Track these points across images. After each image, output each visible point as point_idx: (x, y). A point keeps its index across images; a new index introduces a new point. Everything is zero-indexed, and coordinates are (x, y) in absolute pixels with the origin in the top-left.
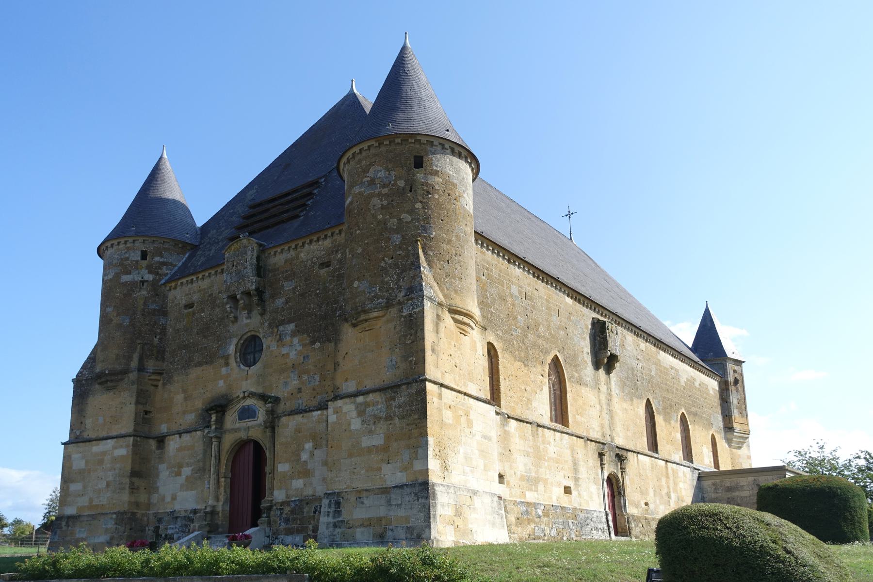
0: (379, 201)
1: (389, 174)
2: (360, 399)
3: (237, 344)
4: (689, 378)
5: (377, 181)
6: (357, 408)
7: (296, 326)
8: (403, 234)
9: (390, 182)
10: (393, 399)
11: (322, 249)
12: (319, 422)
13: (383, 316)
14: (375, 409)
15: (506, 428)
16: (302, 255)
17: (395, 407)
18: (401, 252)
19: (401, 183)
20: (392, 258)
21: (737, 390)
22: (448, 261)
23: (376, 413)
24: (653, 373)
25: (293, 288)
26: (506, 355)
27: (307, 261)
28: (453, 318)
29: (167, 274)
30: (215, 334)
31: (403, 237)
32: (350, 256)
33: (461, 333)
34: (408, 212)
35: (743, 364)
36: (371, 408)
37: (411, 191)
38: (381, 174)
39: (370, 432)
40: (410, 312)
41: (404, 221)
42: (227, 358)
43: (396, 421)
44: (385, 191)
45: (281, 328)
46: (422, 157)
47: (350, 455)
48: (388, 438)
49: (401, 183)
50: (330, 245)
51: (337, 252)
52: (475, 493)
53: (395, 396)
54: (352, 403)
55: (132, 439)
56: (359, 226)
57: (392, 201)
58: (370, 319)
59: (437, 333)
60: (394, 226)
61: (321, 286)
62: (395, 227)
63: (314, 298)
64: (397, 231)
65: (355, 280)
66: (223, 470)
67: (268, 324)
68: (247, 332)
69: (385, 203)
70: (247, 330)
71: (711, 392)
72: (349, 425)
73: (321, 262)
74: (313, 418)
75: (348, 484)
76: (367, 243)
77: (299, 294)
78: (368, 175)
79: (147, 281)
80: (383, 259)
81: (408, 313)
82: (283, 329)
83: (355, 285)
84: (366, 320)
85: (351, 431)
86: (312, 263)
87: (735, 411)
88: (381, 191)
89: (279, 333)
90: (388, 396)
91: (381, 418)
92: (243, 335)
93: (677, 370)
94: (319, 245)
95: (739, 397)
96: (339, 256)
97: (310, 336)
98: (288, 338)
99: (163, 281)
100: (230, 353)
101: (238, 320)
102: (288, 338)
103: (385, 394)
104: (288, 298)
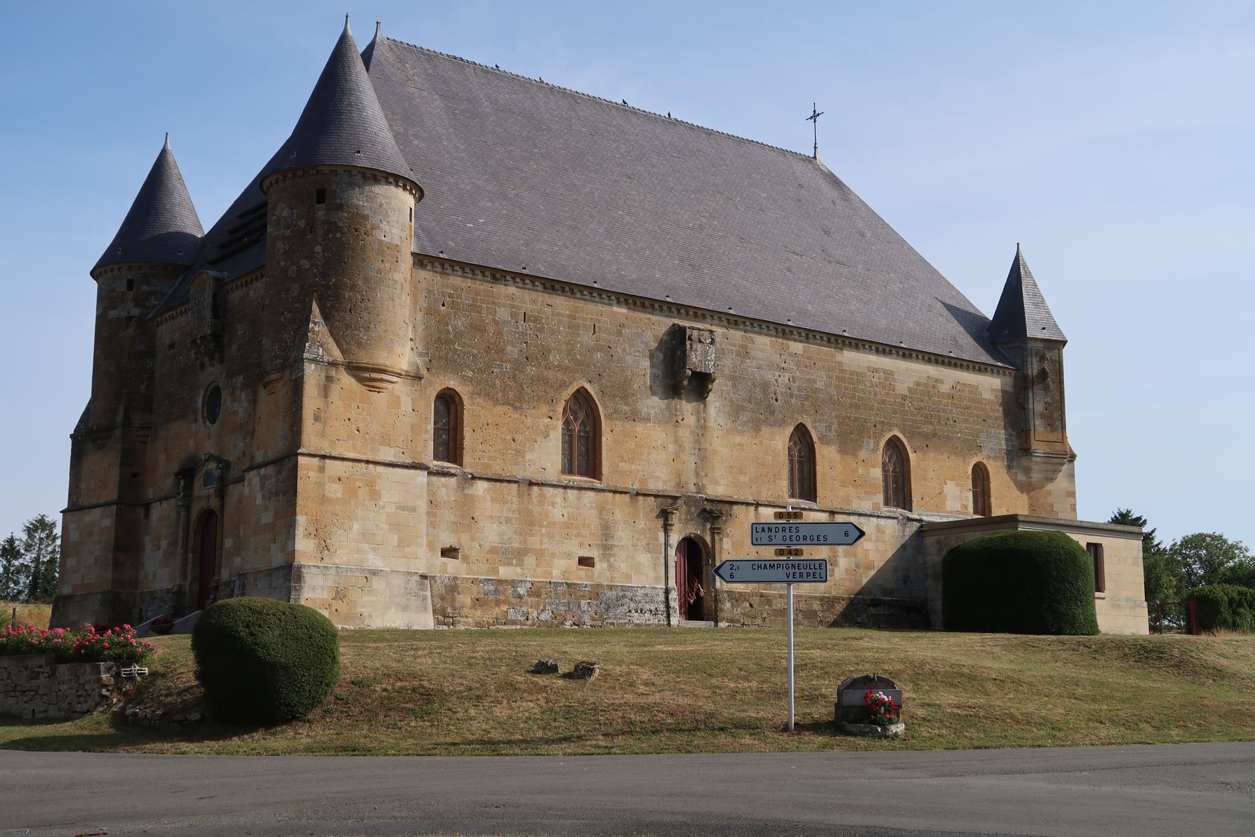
1: (292, 213)
4: (923, 381)
13: (281, 379)
15: (467, 491)
19: (302, 223)
20: (290, 312)
22: (350, 310)
24: (820, 385)
26: (480, 400)
29: (155, 306)
33: (370, 391)
41: (303, 267)
42: (195, 411)
44: (288, 232)
46: (324, 190)
52: (375, 573)
55: (115, 507)
59: (326, 396)
62: (294, 276)
66: (191, 544)
79: (134, 316)
80: (283, 314)
87: (1037, 423)
92: (209, 385)
95: (1049, 400)
99: (150, 316)
102: (238, 392)
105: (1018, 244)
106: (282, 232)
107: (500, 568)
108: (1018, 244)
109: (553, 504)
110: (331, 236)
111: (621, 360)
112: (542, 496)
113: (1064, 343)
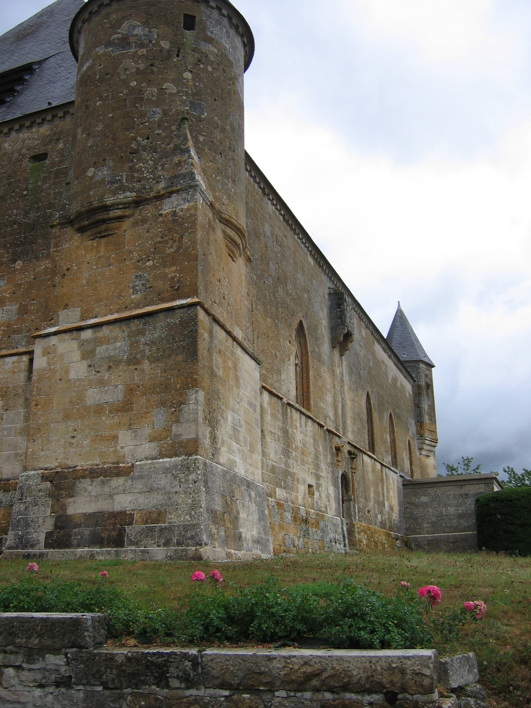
0: (133, 63)
1: (150, 32)
2: (87, 334)
5: (132, 40)
6: (82, 344)
8: (165, 108)
9: (151, 42)
10: (142, 333)
11: (36, 137)
12: (14, 372)
13: (129, 216)
14: (111, 347)
16: (6, 145)
17: (146, 344)
18: (160, 132)
20: (148, 138)
21: (428, 395)
23: (112, 354)
27: (13, 153)
28: (224, 232)
31: (165, 113)
32: (84, 135)
34: (173, 81)
35: (433, 369)
36: (104, 347)
37: (178, 56)
38: (139, 31)
39: (101, 383)
40: (174, 210)
41: (167, 91)
43: (146, 365)
46: (194, 17)
47: (67, 417)
48: (130, 391)
49: (165, 45)
50: (48, 133)
51: (58, 140)
53: (145, 328)
54: (73, 339)
56: (101, 97)
57: (152, 65)
58: (110, 219)
60: (153, 96)
61: (30, 186)
63: (18, 201)
64: (157, 104)
65: (89, 167)
69: (142, 66)
71: (407, 395)
72: (67, 372)
73: (33, 154)
75: (60, 461)
76: (112, 117)
78: (119, 31)
80: (135, 139)
81: (171, 210)
83: (90, 173)
84: (104, 221)
85: (69, 380)
86: (20, 155)
88: (137, 51)
90: (134, 328)
91: (120, 361)
93: (386, 366)
94: (32, 133)
95: (429, 403)
96: (61, 146)
97: (8, 253)
103: (129, 327)
105: (399, 302)
106: (133, 50)
107: (277, 489)
108: (399, 302)
109: (296, 428)
110: (202, 66)
111: (313, 306)
112: (291, 417)
113: (434, 366)
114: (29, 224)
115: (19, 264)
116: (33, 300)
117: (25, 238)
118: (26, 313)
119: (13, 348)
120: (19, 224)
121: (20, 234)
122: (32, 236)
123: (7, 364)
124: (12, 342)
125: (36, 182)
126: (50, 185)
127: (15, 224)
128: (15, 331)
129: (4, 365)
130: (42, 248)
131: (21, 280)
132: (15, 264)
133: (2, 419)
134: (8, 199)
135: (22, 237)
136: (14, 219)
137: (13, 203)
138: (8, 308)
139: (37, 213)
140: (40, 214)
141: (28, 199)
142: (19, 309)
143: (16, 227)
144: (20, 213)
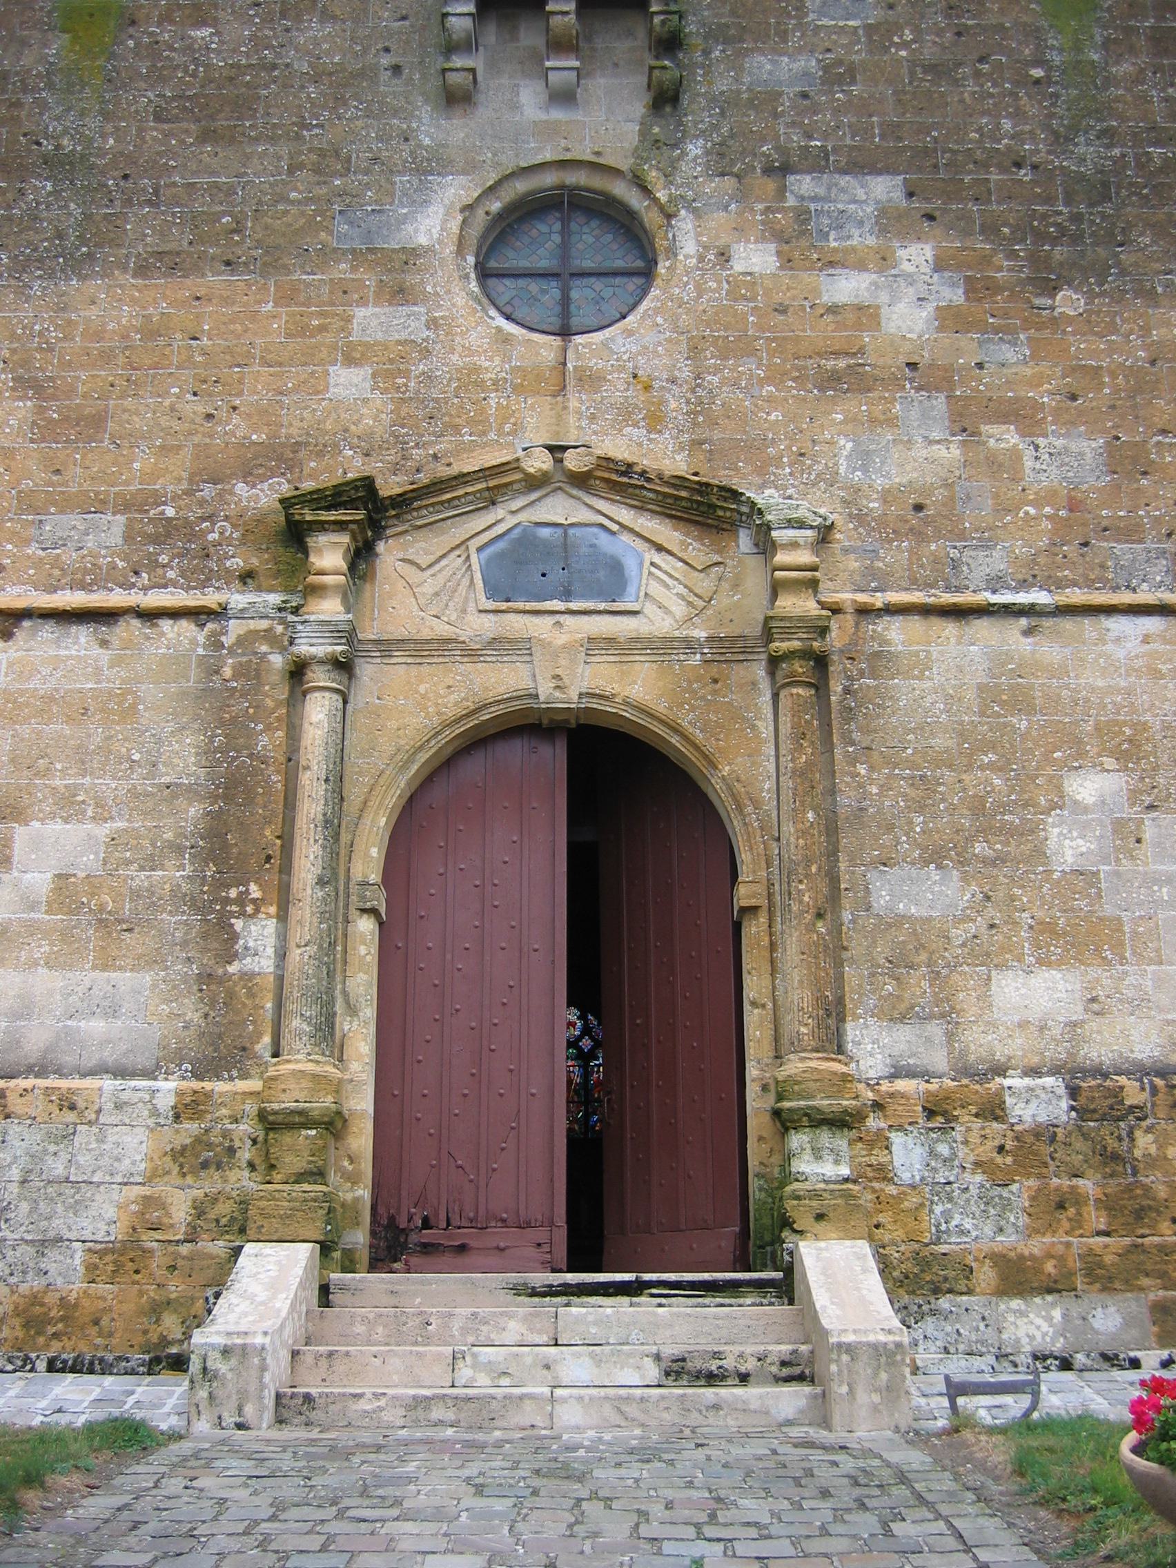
3: (469, 208)
7: (910, 195)
25: (869, 29)
30: (298, 137)
45: (804, 184)
67: (707, 153)
68: (543, 166)
70: (548, 156)
74: (1110, 647)
77: (913, 63)
82: (821, 191)
89: (791, 201)
97: (1013, 255)
98: (862, 239)
100: (423, 240)
101: (481, 98)
104: (839, 62)
114: (1081, 177)
115: (1068, 302)
116: (1164, 432)
117: (1077, 218)
118: (1145, 473)
119: (1115, 589)
120: (1035, 167)
121: (1049, 200)
122: (1104, 216)
123: (1118, 640)
124: (1103, 566)
125: (1077, 48)
126: (1142, 71)
127: (1019, 165)
128: (1105, 529)
129: (1102, 640)
130: (1157, 266)
131: (1095, 354)
132: (1053, 297)
133: (1139, 841)
134: (964, 79)
135: (1060, 213)
136: (1008, 147)
137: (991, 96)
138: (1060, 443)
139: (1109, 146)
140: (1123, 156)
141: (1056, 96)
142: (1110, 455)
143: (1025, 174)
144: (1031, 132)
